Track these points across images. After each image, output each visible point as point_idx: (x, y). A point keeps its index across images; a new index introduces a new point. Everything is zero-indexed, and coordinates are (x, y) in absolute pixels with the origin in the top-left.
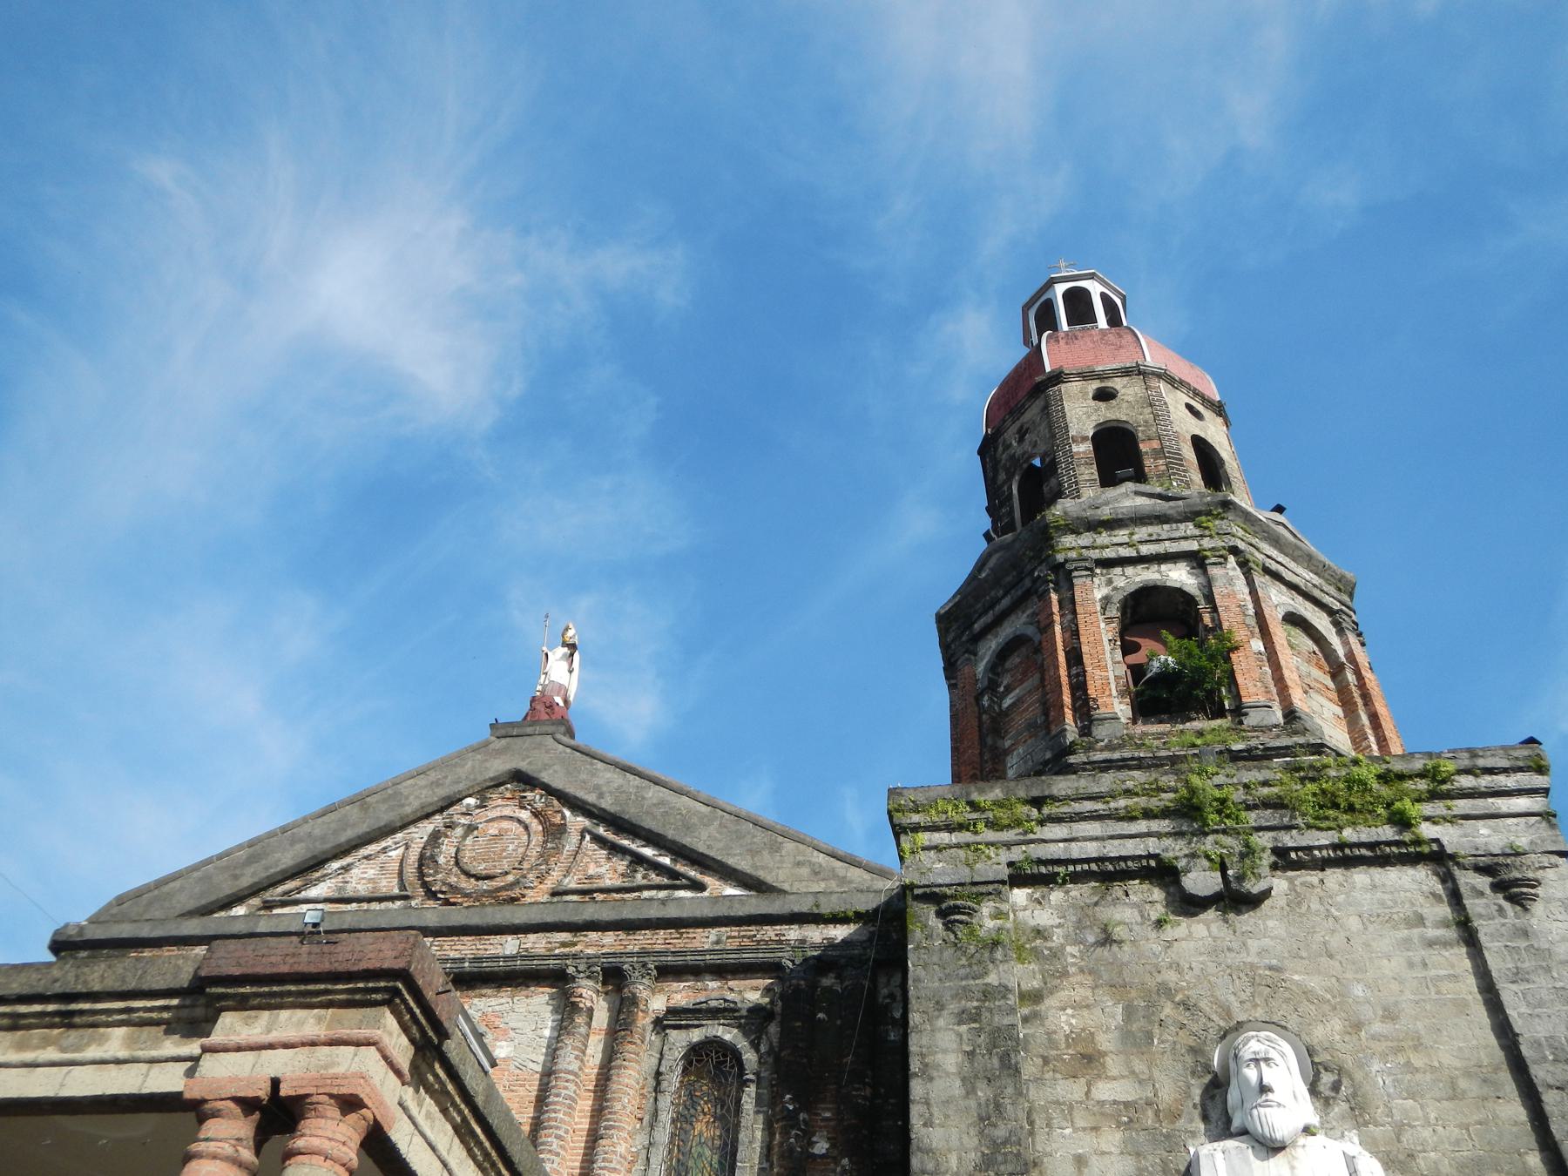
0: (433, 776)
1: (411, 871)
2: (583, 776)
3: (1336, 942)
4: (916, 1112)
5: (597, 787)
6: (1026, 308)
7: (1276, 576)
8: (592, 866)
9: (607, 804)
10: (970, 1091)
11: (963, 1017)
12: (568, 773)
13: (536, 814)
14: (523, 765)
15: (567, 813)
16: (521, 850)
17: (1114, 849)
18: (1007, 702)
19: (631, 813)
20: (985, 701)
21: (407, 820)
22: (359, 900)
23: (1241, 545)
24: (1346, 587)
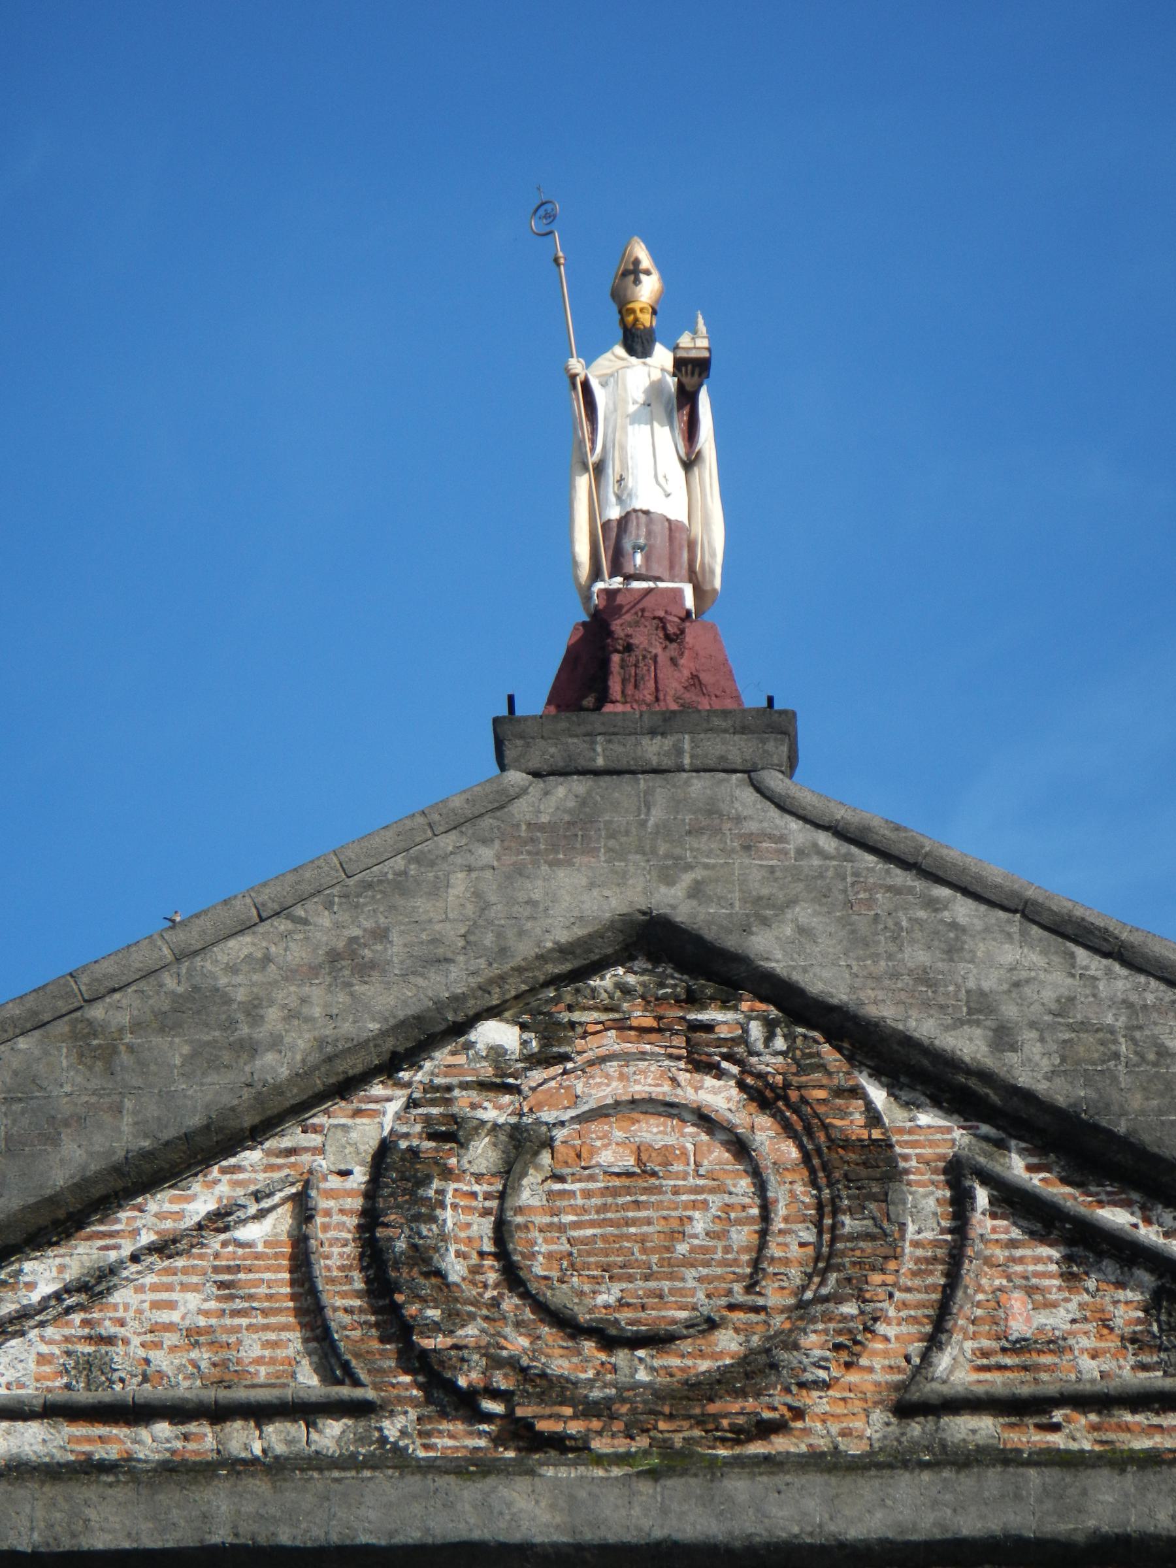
0: (326, 926)
1: (344, 1300)
2: (917, 956)
5: (980, 1006)
8: (1017, 1302)
9: (1032, 1068)
12: (857, 941)
13: (763, 1095)
14: (673, 900)
15: (878, 1095)
16: (743, 1236)
21: (275, 1106)
22: (178, 1412)
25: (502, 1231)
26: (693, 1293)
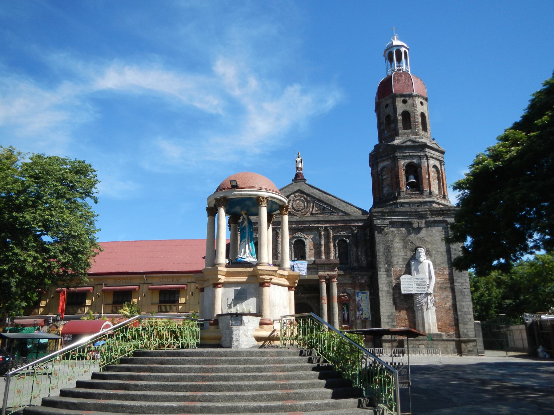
3: (431, 234)
4: (378, 257)
5: (314, 194)
6: (386, 50)
7: (432, 157)
10: (384, 254)
11: (383, 244)
14: (301, 189)
17: (404, 220)
18: (384, 178)
19: (322, 198)
23: (427, 154)
24: (443, 153)
26: (301, 208)
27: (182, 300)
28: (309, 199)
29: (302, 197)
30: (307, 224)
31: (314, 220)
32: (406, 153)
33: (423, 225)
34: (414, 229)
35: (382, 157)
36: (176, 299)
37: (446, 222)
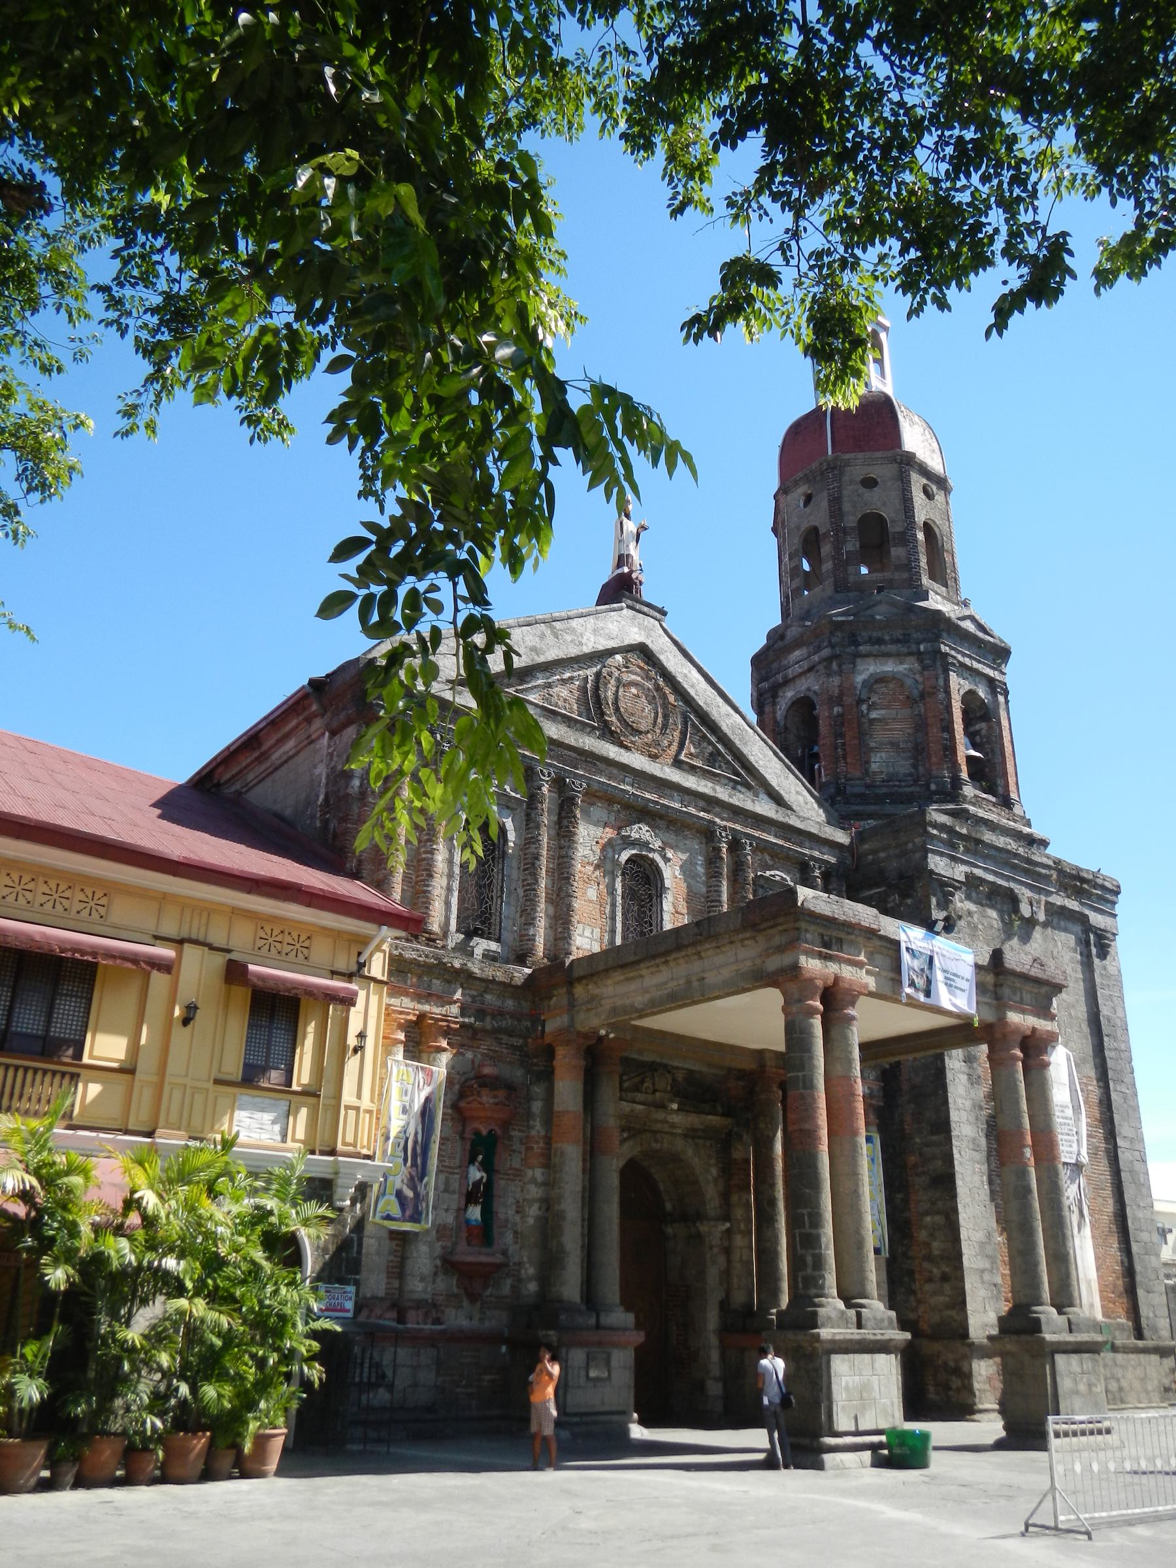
14: (648, 642)
17: (1000, 882)
20: (864, 707)
25: (616, 699)
27: (106, 1047)
28: (671, 698)
29: (649, 678)
30: (672, 798)
31: (701, 789)
32: (964, 655)
33: (1041, 917)
34: (1022, 918)
35: (879, 641)
36: (56, 1031)
37: (1083, 919)
